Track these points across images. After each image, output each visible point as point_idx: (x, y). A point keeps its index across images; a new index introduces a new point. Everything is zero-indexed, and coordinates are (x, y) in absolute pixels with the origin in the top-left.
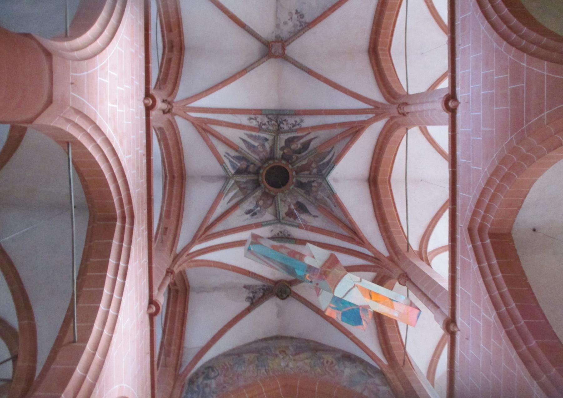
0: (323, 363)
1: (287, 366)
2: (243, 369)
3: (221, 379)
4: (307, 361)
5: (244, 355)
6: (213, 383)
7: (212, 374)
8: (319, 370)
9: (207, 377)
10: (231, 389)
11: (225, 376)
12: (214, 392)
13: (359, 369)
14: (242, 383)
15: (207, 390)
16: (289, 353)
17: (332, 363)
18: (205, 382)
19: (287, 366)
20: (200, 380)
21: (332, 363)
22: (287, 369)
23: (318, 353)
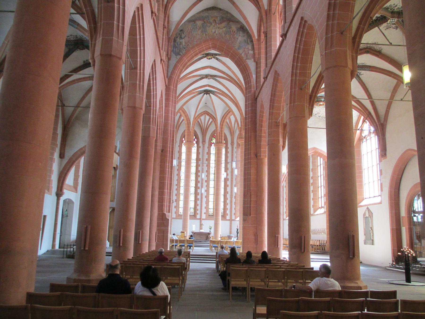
0: (230, 31)
1: (215, 32)
2: (196, 33)
3: (187, 38)
4: (224, 29)
5: (197, 22)
6: (183, 41)
7: (183, 36)
8: (228, 36)
9: (181, 38)
10: (191, 46)
11: (189, 37)
12: (184, 48)
13: (245, 38)
14: (195, 43)
15: (181, 46)
16: (217, 22)
17: (235, 32)
18: (180, 41)
19: (215, 32)
20: (178, 39)
21: (235, 32)
22: (215, 34)
23: (231, 23)
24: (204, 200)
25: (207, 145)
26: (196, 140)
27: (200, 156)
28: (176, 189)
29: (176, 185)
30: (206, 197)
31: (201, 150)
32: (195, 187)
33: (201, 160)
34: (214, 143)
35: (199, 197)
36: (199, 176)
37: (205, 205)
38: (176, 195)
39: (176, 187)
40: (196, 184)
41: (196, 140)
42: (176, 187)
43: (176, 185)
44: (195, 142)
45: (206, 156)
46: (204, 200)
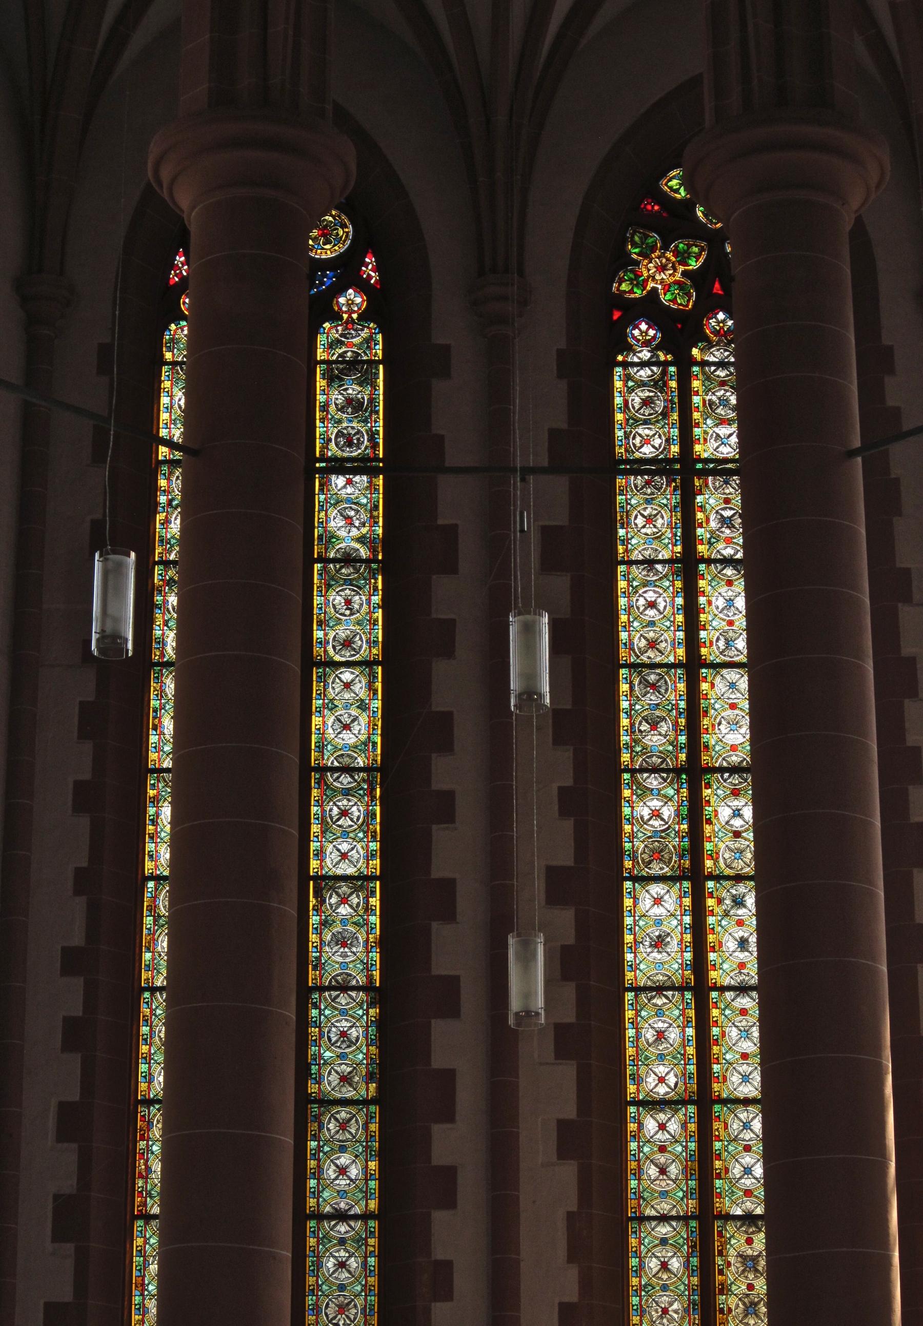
24: (549, 1188)
25: (545, 332)
26: (370, 271)
27: (456, 503)
28: (75, 1034)
29: (72, 962)
30: (570, 1140)
31: (454, 409)
32: (376, 994)
33: (469, 548)
34: (650, 307)
35: (456, 1143)
36: (445, 808)
37: (567, 1285)
38: (71, 1123)
39: (70, 997)
40: (401, 941)
41: (370, 271)
42: (70, 997)
43: (72, 962)
44: (352, 300)
45: (538, 505)
46: (549, 1188)
